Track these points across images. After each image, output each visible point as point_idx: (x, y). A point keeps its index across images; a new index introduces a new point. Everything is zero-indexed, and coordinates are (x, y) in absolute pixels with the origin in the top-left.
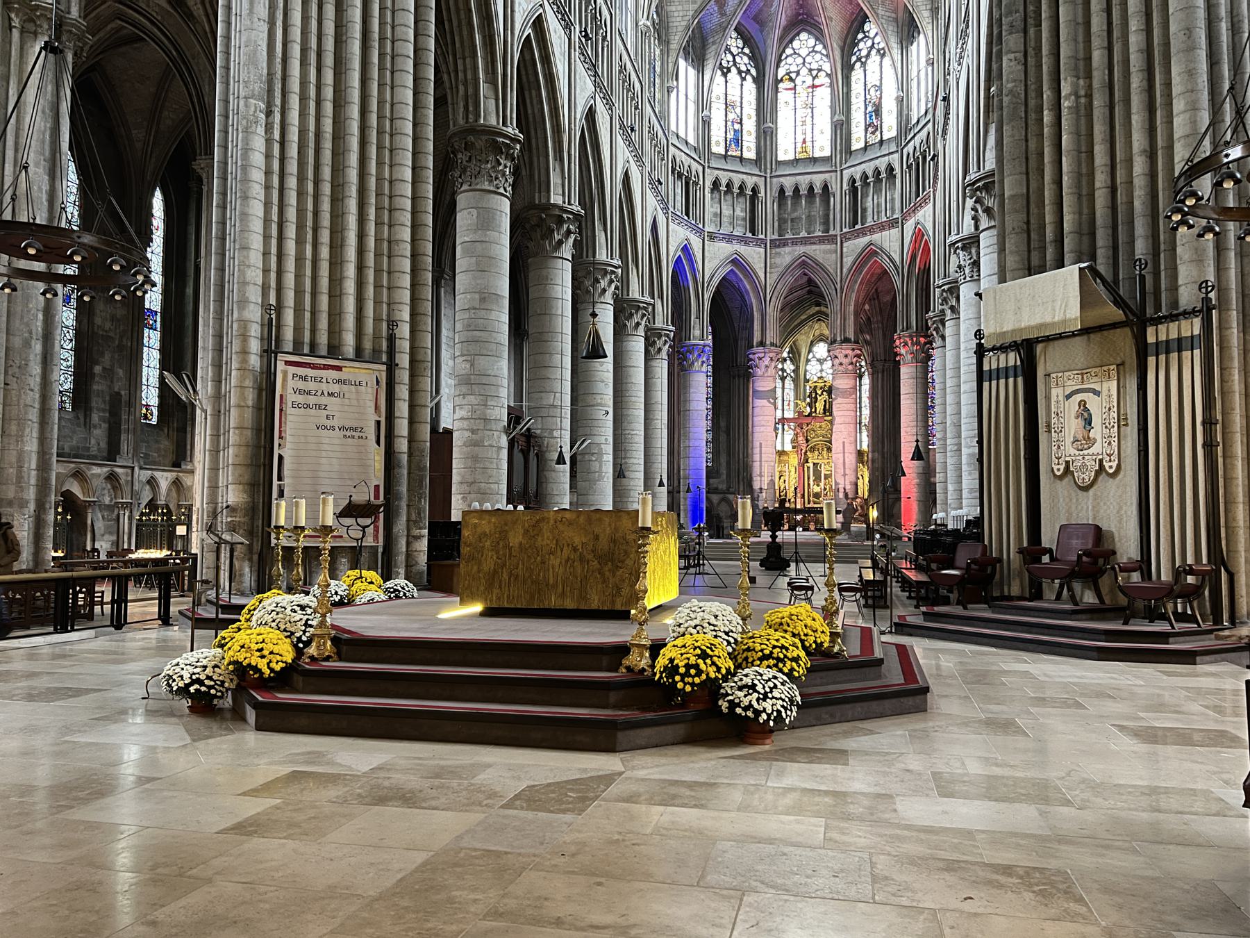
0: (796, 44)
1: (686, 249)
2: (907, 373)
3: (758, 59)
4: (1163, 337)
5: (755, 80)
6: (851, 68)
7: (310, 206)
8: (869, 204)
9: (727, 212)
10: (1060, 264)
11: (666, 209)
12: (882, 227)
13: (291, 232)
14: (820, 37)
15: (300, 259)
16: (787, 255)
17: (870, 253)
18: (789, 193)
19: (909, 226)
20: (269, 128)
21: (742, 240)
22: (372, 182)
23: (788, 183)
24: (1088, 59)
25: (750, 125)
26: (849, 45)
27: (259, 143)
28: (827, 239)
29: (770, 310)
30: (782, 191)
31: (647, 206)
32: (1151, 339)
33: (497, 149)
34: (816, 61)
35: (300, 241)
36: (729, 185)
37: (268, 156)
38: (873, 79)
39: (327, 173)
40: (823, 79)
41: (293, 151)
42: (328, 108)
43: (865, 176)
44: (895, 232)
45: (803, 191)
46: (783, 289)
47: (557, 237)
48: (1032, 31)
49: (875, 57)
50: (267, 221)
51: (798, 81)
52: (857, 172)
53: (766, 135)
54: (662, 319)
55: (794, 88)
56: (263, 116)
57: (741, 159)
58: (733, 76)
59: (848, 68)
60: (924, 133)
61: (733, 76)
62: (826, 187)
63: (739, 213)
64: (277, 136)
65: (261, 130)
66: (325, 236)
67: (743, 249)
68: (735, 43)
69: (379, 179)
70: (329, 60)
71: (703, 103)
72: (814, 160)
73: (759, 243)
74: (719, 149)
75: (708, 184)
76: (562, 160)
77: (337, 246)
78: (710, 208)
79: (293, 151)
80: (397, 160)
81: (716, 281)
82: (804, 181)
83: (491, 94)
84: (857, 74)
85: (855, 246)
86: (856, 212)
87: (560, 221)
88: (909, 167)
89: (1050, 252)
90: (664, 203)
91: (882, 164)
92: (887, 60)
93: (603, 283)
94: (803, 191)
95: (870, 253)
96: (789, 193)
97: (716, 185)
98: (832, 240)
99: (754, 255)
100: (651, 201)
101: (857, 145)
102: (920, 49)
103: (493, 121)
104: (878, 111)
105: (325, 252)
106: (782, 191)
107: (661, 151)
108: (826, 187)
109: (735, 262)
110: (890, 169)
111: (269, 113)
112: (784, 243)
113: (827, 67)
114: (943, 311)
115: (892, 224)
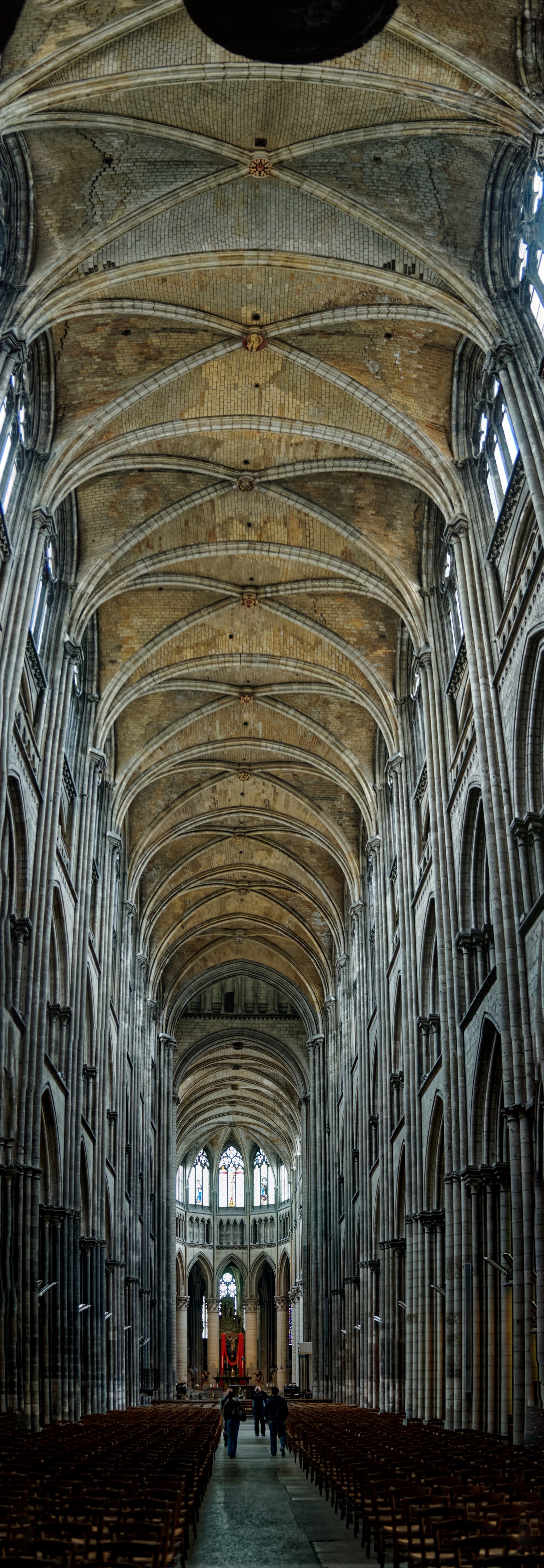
14: (238, 1148)
18: (225, 1223)
26: (253, 1157)
28: (243, 1247)
34: (238, 1161)
38: (264, 1175)
40: (240, 1170)
45: (232, 1223)
49: (264, 1166)
52: (257, 1217)
62: (242, 1222)
72: (236, 1208)
94: (232, 1223)
96: (225, 1223)
108: (242, 1222)
112: (222, 1248)
113: (242, 1164)
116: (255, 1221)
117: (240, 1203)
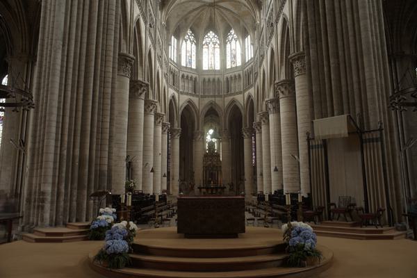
0: (209, 34)
1: (173, 97)
2: (246, 141)
3: (196, 37)
4: (368, 137)
5: (196, 44)
6: (226, 43)
7: (76, 79)
8: (233, 85)
9: (186, 85)
10: (333, 115)
11: (167, 83)
12: (237, 93)
13: (69, 88)
14: (216, 32)
15: (72, 98)
16: (206, 101)
17: (233, 101)
18: (207, 80)
19: (246, 94)
20: (63, 51)
21: (191, 94)
22: (99, 72)
23: (207, 77)
24: (338, 53)
25: (194, 58)
27: (59, 56)
29: (200, 118)
30: (204, 80)
31: (163, 82)
32: (364, 138)
33: (127, 61)
34: (215, 40)
35: (72, 92)
36: (187, 76)
37: (62, 61)
38: (233, 47)
39: (83, 68)
40: (217, 46)
41: (72, 60)
42: (85, 45)
43: (231, 78)
44: (241, 95)
45: (211, 80)
46: (205, 112)
47: (140, 91)
48: (318, 43)
49: (233, 41)
50: (61, 84)
51: (210, 45)
52: (229, 75)
53: (199, 62)
54: (166, 119)
55: (208, 48)
56: (61, 47)
57: (191, 68)
58: (189, 42)
59: (225, 43)
60: (250, 65)
61: (189, 42)
62: (218, 79)
63: (190, 86)
64: (66, 53)
65: (61, 51)
66: (81, 90)
67: (191, 98)
68: (189, 32)
69: (101, 71)
70: (86, 29)
71: (179, 50)
72: (215, 71)
73: (197, 96)
74: (183, 64)
75: (181, 76)
76: (142, 66)
77: (85, 94)
78: (181, 84)
79: (72, 60)
80: (107, 65)
81: (182, 108)
82: (212, 77)
83: (125, 43)
84: (228, 45)
85: (228, 99)
86: (228, 89)
87: (141, 86)
88: (246, 75)
89: (329, 110)
90: (167, 81)
91: (237, 73)
92: (238, 42)
93: (151, 108)
94: (211, 80)
95: (233, 101)
96: (207, 80)
97: (183, 76)
98: (221, 96)
99: (195, 100)
100: (164, 80)
101: (228, 66)
102: (248, 40)
103: (125, 52)
104: (235, 57)
105: (81, 96)
106: (204, 80)
107: (167, 64)
108: (218, 79)
109: (189, 102)
110: (239, 75)
111: (63, 46)
112: (205, 97)
113: (218, 42)
114: (261, 123)
115: (240, 93)
116: (227, 78)
117: (218, 67)
